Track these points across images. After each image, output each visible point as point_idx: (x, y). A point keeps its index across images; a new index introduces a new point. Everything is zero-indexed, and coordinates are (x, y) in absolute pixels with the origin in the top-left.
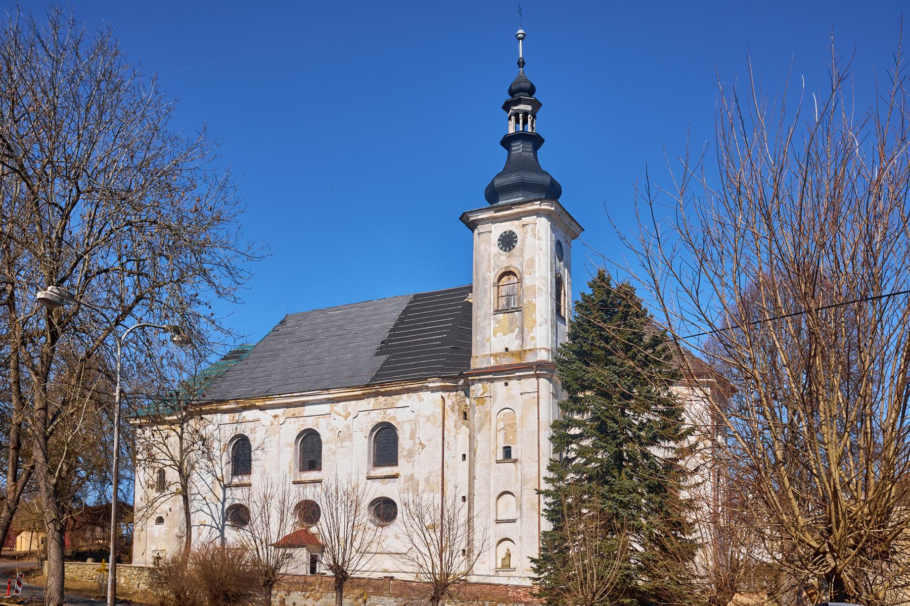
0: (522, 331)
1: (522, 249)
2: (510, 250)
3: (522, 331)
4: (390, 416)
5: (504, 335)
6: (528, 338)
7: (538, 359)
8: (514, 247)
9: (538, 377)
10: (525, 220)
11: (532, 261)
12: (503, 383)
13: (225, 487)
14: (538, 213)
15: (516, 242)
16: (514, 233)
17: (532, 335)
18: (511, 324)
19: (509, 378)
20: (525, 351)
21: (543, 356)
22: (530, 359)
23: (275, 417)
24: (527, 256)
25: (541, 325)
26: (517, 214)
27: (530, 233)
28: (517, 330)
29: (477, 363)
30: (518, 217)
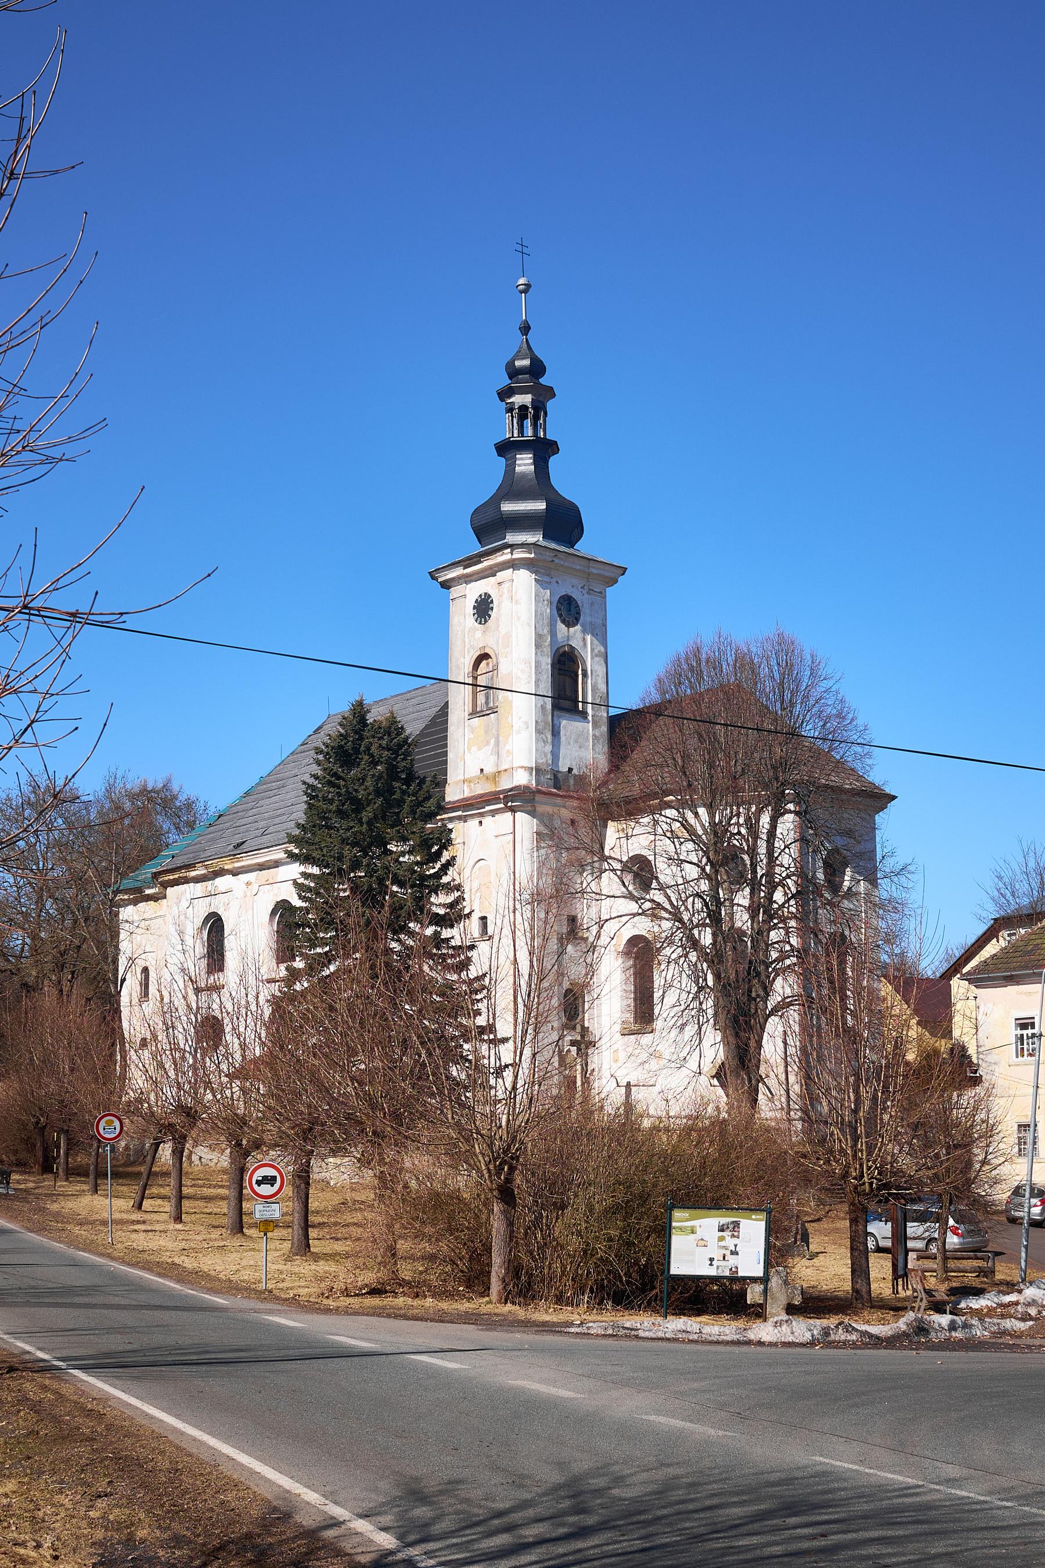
0: (497, 743)
1: (498, 619)
2: (486, 622)
3: (497, 743)
4: (218, 905)
5: (480, 749)
6: (503, 752)
7: (515, 783)
8: (490, 616)
9: (513, 810)
10: (501, 575)
11: (508, 636)
12: (476, 821)
13: (198, 991)
14: (513, 565)
15: (492, 609)
16: (490, 596)
17: (508, 747)
18: (486, 732)
19: (482, 815)
20: (499, 772)
21: (522, 779)
22: (505, 784)
23: (248, 884)
24: (503, 630)
25: (519, 733)
26: (490, 567)
27: (506, 595)
28: (492, 741)
29: (453, 794)
30: (492, 572)
